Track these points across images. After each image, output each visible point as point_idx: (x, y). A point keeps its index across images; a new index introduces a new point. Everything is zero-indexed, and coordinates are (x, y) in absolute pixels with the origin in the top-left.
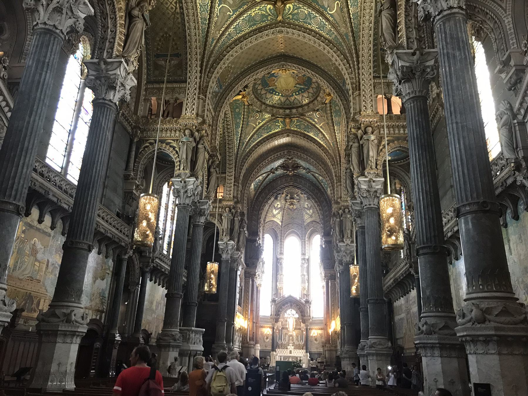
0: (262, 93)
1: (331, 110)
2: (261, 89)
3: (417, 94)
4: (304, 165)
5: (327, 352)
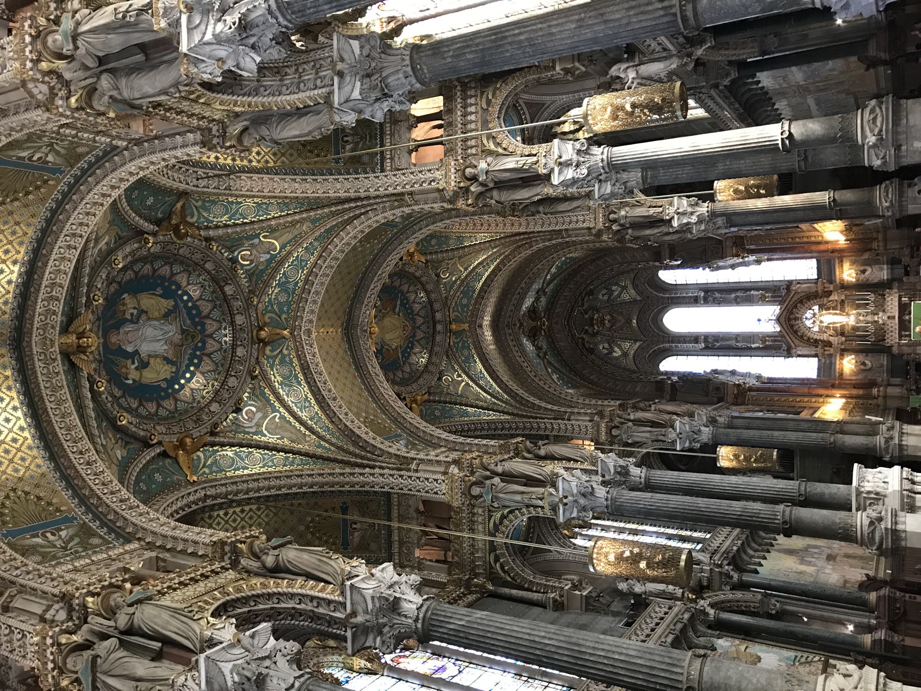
0: (408, 370)
1: (436, 252)
2: (403, 371)
3: (408, 62)
4: (532, 300)
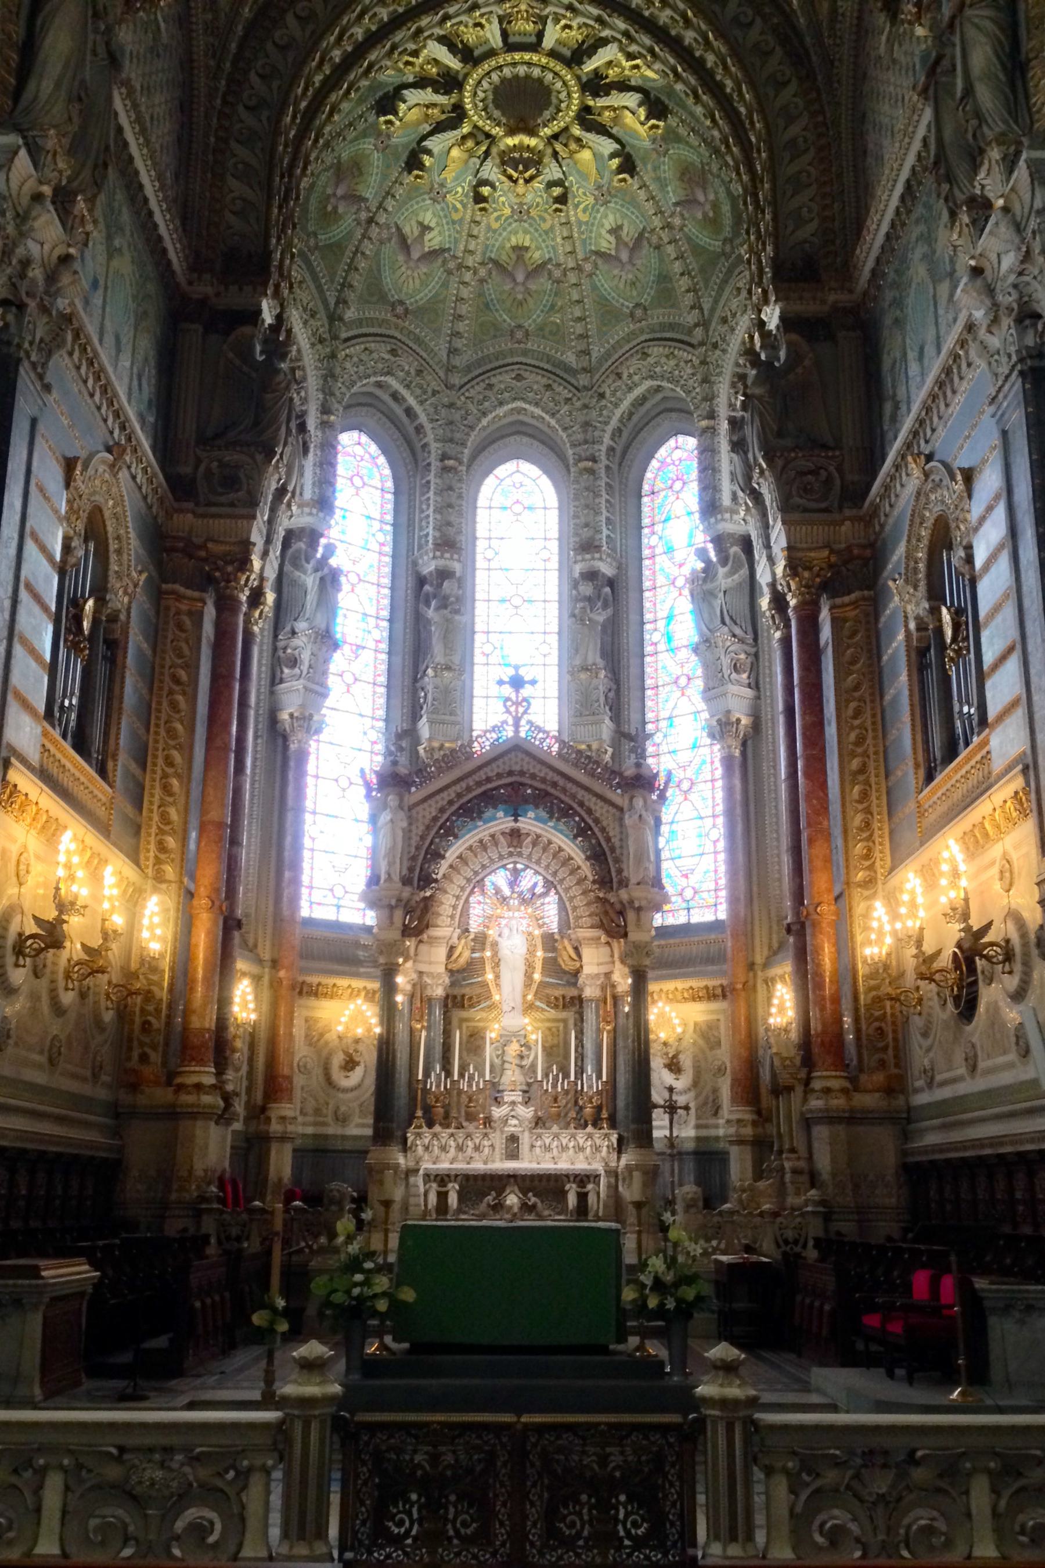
5: (821, 1132)
